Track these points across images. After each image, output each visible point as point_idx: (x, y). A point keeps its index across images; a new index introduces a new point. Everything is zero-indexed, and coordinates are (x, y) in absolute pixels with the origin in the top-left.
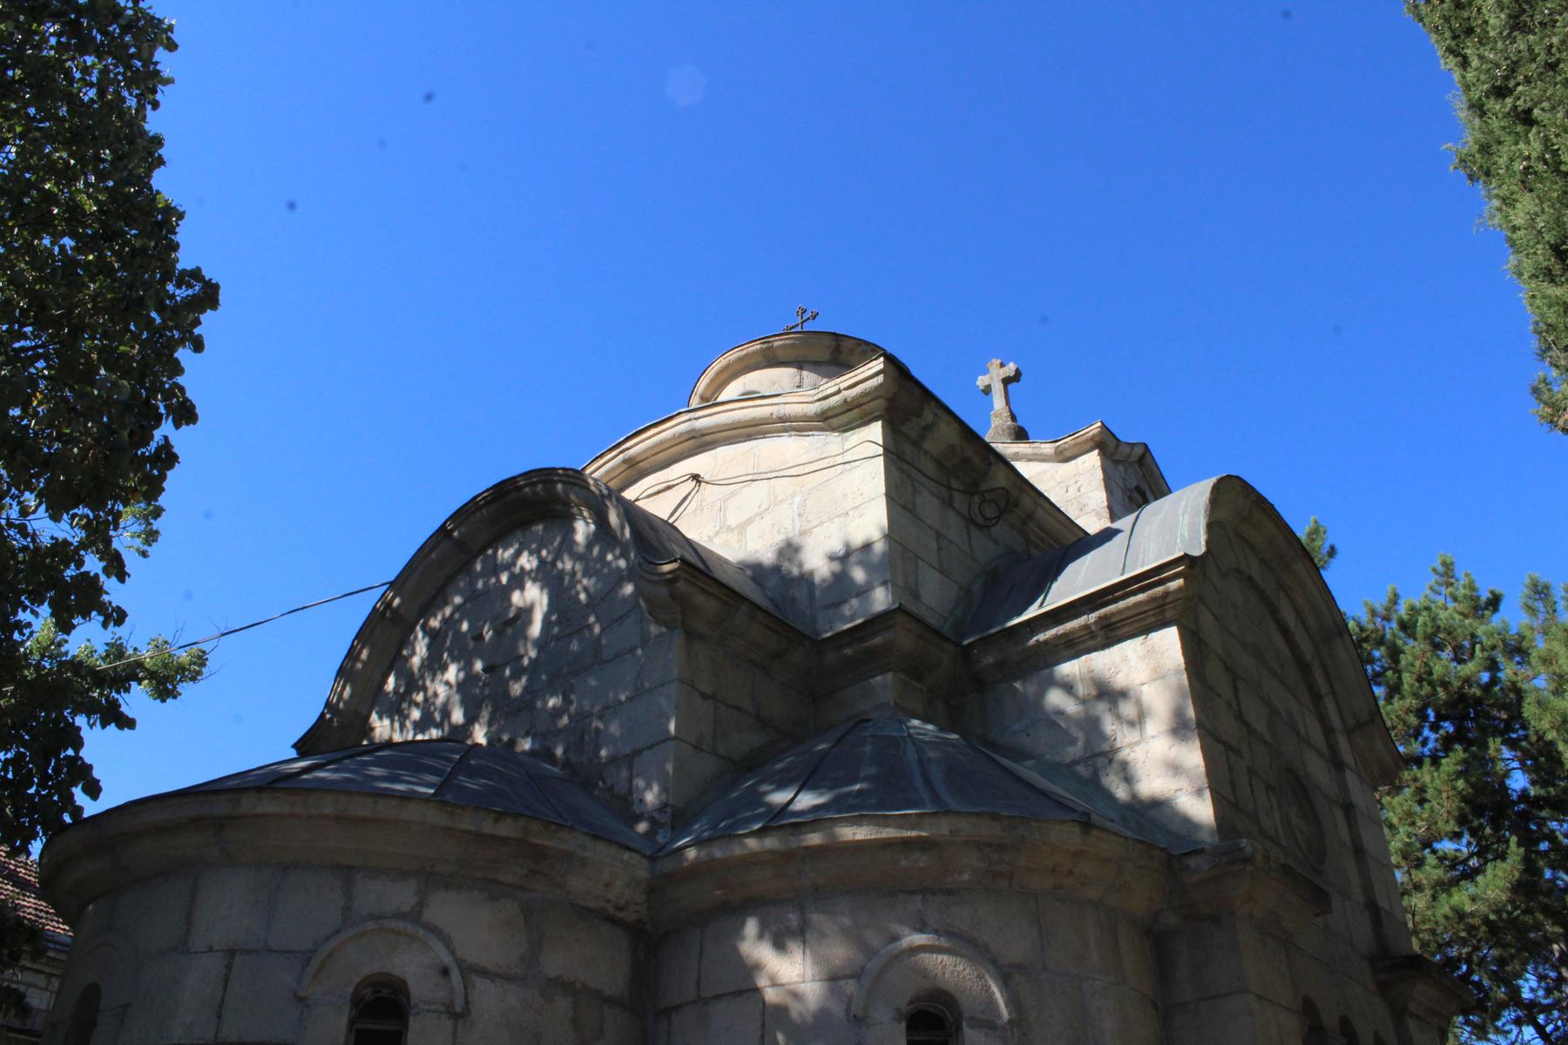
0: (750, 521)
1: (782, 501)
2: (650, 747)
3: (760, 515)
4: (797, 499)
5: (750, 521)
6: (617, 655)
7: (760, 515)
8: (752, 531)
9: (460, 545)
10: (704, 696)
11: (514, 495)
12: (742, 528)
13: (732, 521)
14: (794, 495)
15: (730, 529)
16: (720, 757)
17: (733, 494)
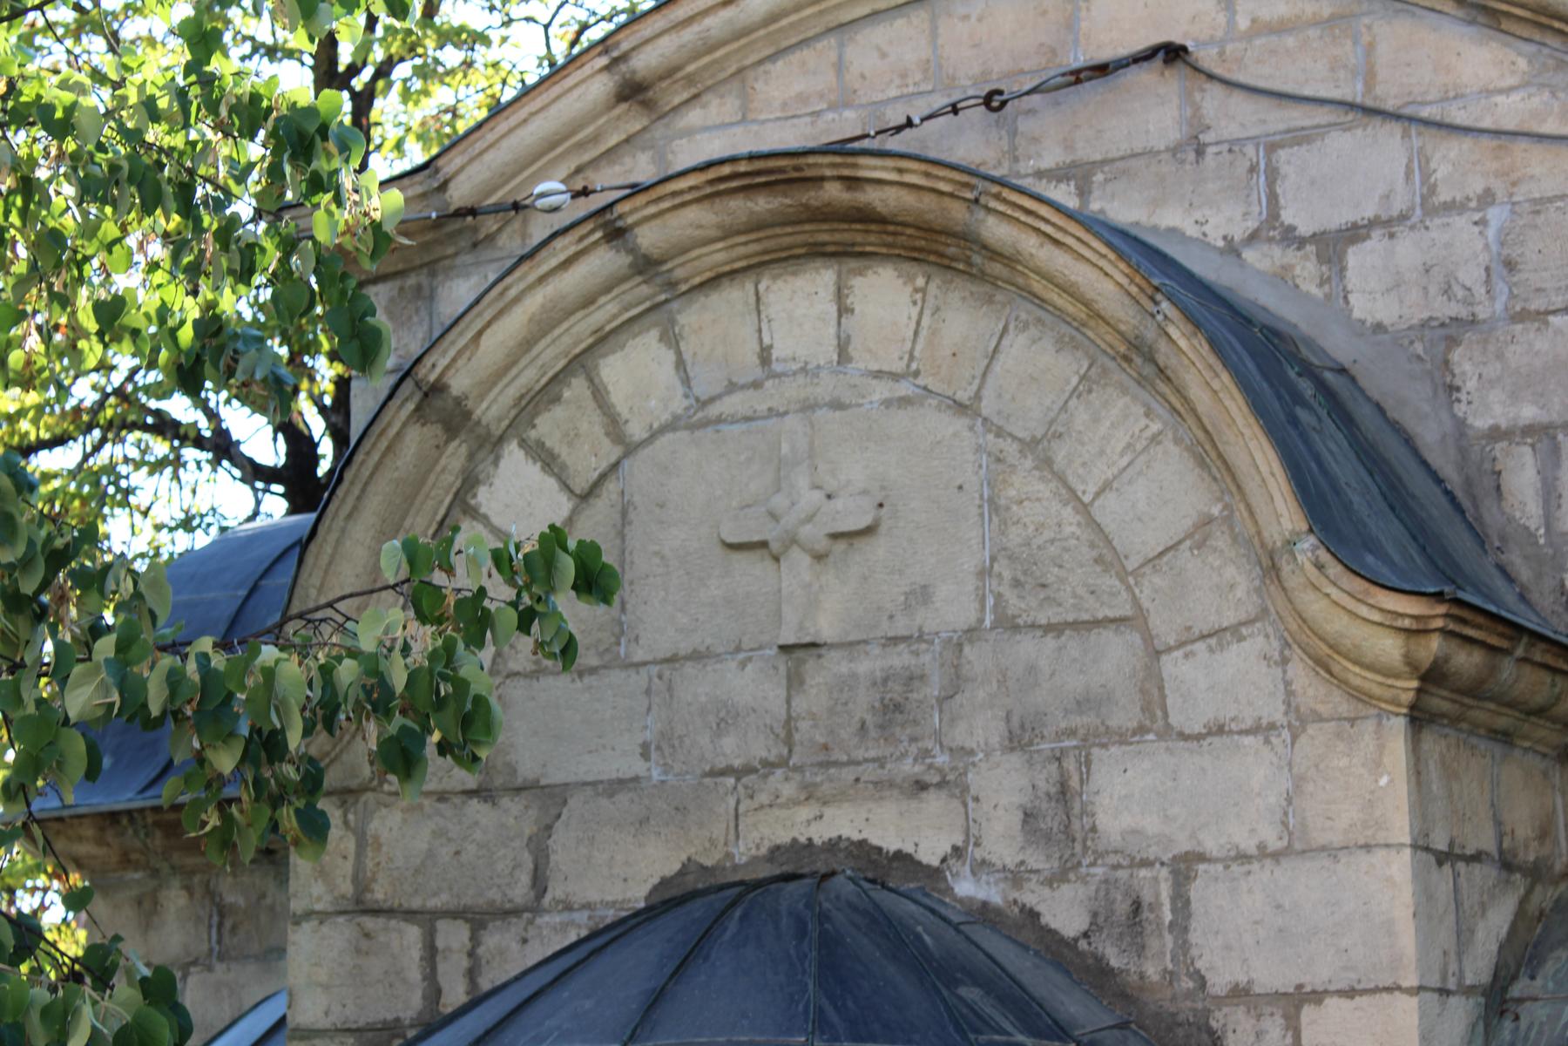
0: (1355, 233)
1: (1450, 207)
2: (1350, 993)
3: (1387, 224)
4: (1497, 216)
5: (1355, 233)
6: (1220, 730)
7: (1387, 224)
8: (1355, 257)
9: (646, 266)
10: (1442, 858)
11: (833, 192)
12: (1333, 246)
13: (1300, 216)
14: (1487, 198)
15: (1290, 237)
16: (1469, 991)
17: (1300, 137)
